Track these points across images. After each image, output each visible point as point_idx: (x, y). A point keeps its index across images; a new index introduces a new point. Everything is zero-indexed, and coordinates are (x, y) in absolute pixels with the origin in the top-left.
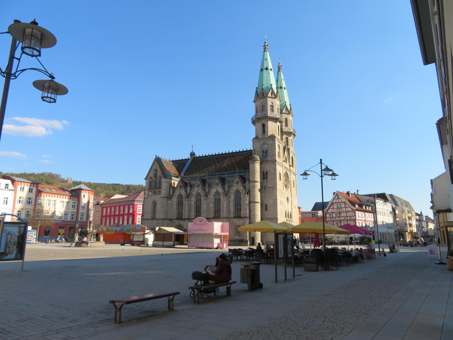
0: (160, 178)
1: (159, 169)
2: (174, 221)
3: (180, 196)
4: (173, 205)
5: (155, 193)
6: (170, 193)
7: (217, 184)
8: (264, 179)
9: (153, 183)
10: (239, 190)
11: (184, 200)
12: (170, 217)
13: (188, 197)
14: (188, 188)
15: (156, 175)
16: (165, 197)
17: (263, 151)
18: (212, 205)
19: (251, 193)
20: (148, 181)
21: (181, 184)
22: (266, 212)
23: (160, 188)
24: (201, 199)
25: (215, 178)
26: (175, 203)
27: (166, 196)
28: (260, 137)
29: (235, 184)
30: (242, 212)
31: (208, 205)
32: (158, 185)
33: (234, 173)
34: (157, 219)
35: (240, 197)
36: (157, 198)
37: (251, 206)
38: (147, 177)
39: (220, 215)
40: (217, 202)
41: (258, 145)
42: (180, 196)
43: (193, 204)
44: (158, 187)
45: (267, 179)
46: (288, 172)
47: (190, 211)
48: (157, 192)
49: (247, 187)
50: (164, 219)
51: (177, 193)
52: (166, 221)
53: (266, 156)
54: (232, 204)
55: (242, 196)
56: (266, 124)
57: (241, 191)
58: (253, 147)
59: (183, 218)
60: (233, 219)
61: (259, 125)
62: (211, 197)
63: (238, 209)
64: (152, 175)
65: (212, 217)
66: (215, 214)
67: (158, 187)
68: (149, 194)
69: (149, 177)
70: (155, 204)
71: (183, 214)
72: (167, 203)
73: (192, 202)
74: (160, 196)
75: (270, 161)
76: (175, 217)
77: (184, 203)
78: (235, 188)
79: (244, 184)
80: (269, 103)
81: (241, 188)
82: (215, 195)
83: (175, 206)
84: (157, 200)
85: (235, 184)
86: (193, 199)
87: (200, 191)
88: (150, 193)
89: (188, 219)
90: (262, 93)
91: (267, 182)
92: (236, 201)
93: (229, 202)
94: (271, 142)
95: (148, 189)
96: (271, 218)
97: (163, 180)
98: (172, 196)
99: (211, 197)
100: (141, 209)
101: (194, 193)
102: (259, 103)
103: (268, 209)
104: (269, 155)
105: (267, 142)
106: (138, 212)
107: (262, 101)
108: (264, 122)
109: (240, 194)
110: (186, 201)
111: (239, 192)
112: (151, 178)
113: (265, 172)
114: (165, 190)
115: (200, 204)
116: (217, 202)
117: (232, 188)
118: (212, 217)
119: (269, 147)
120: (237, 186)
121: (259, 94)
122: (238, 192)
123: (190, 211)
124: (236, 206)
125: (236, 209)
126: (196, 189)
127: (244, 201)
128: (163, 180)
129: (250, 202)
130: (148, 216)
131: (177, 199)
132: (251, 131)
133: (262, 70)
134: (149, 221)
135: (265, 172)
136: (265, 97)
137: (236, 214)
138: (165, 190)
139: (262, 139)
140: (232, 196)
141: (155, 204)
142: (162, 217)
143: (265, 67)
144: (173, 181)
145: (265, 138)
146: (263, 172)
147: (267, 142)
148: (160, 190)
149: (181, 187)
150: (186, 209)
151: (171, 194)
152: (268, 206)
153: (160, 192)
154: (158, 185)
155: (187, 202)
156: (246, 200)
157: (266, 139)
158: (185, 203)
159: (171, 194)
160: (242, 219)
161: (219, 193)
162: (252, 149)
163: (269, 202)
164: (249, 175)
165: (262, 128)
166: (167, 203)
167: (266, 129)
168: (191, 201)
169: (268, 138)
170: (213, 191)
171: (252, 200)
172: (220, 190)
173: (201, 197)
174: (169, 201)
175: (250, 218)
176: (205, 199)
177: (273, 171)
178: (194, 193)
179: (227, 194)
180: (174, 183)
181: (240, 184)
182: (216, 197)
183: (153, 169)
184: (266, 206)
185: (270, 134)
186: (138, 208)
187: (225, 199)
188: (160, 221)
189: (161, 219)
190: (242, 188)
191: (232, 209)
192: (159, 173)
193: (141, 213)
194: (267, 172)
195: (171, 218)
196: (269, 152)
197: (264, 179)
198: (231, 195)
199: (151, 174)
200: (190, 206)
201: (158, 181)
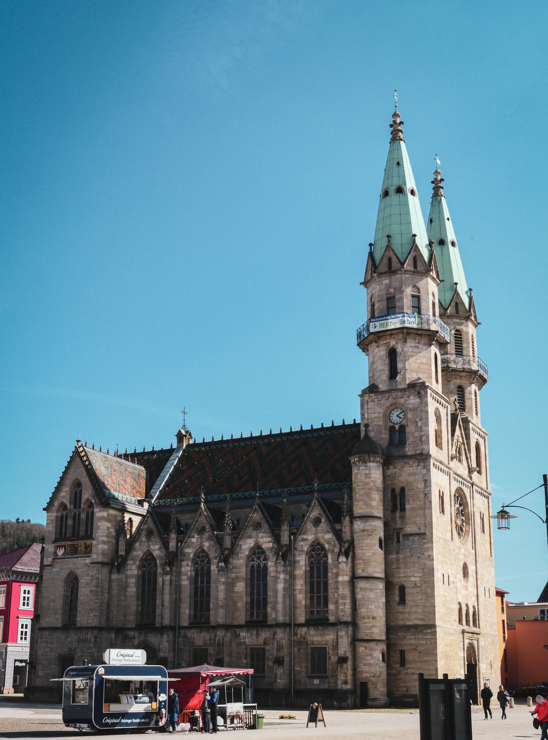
0: (91, 506)
1: (85, 481)
2: (131, 633)
3: (149, 558)
4: (127, 586)
5: (74, 552)
6: (117, 551)
7: (257, 526)
8: (394, 510)
9: (70, 522)
10: (322, 541)
11: (159, 570)
12: (117, 622)
13: (170, 564)
14: (173, 536)
15: (76, 497)
16: (103, 564)
17: (392, 429)
18: (240, 587)
19: (358, 552)
21: (150, 524)
22: (401, 608)
23: (89, 535)
24: (209, 569)
25: (251, 507)
26: (133, 581)
27: (105, 560)
28: (382, 387)
29: (309, 525)
30: (331, 607)
31: (230, 586)
32: (82, 528)
33: (306, 493)
34: (80, 629)
35: (326, 562)
36: (80, 565)
37: (358, 590)
38: (50, 504)
39: (265, 615)
40: (258, 578)
41: (376, 411)
42: (149, 558)
43: (185, 583)
44: (82, 533)
45: (403, 509)
46: (464, 488)
47: (176, 603)
48: (82, 548)
49: (347, 536)
50: (100, 629)
51: (139, 552)
52: (105, 634)
53: (402, 442)
54: (300, 584)
55: (330, 561)
56: (399, 350)
57: (326, 546)
58: (363, 415)
59: (158, 625)
60: (304, 629)
61: (380, 352)
62: (240, 562)
63: (319, 597)
64: (65, 496)
65: (243, 622)
66: (252, 614)
67: (82, 533)
68: (55, 554)
69: (56, 504)
70: (73, 581)
71: (158, 612)
72: (110, 581)
73: (184, 577)
74: (88, 561)
75: (411, 457)
76: (132, 620)
77: (160, 580)
78: (310, 537)
79: (338, 527)
80: (409, 291)
81: (327, 537)
82: (250, 558)
83: (132, 590)
84: (79, 572)
85: (309, 525)
86: (187, 569)
87: (206, 544)
88: (60, 552)
89: (171, 628)
90: (385, 261)
91: (403, 518)
92: (312, 576)
93: (292, 577)
94: (413, 401)
95: (53, 537)
96: (416, 627)
97: (100, 513)
98: (125, 559)
99: (240, 562)
100: (32, 596)
101: (190, 551)
102: (379, 287)
103: (408, 598)
104: (410, 440)
105: (402, 401)
106: (21, 607)
107: (386, 281)
108: (393, 343)
109: (326, 556)
110: (166, 573)
111: (323, 548)
112: (63, 506)
113: (398, 491)
114: (104, 542)
115: (209, 582)
116: (258, 578)
117: (300, 537)
118: (243, 622)
119: (410, 415)
120: (316, 533)
121: (377, 261)
122: (317, 549)
123: (176, 603)
124: (312, 591)
125: (312, 598)
126: (194, 540)
127: (337, 575)
128: (100, 513)
129: (354, 578)
130: (54, 619)
131: (139, 568)
132: (359, 369)
133: (386, 194)
134: (58, 634)
135: (398, 491)
136: (395, 272)
137: (312, 612)
138: (104, 542)
139: (389, 391)
140: (302, 560)
141: (73, 581)
142: (95, 623)
143: (396, 183)
144: (127, 516)
145: (397, 390)
146: (393, 490)
147: (402, 401)
148: (88, 542)
149: (150, 534)
150: (167, 597)
151: (122, 553)
152: (407, 591)
153: (88, 550)
154: (82, 528)
155: (168, 578)
156: (340, 572)
157: (399, 394)
158: (164, 580)
159: (122, 553)
160: (330, 628)
161: (263, 552)
162: (358, 421)
163: (410, 576)
164: (351, 498)
165: (387, 361)
166: (110, 581)
167: (400, 365)
168: (179, 573)
169: (404, 390)
170: (247, 545)
171: (359, 572)
172: (266, 542)
173: (209, 562)
174: (114, 576)
175: (354, 624)
176: (221, 570)
177: (421, 486)
178: (190, 551)
179: (285, 554)
180: (130, 520)
181: (324, 525)
182: (255, 564)
183: (69, 482)
184: (402, 589)
185: (411, 377)
186: (22, 595)
187: (281, 569)
188: (89, 635)
189: (93, 628)
190: (329, 536)
191: (301, 598)
192: (87, 494)
193: (31, 608)
194: (403, 490)
195: (120, 625)
196: (408, 429)
197: (394, 510)
198: (298, 558)
199: (62, 494)
200: (177, 589)
201: (83, 516)
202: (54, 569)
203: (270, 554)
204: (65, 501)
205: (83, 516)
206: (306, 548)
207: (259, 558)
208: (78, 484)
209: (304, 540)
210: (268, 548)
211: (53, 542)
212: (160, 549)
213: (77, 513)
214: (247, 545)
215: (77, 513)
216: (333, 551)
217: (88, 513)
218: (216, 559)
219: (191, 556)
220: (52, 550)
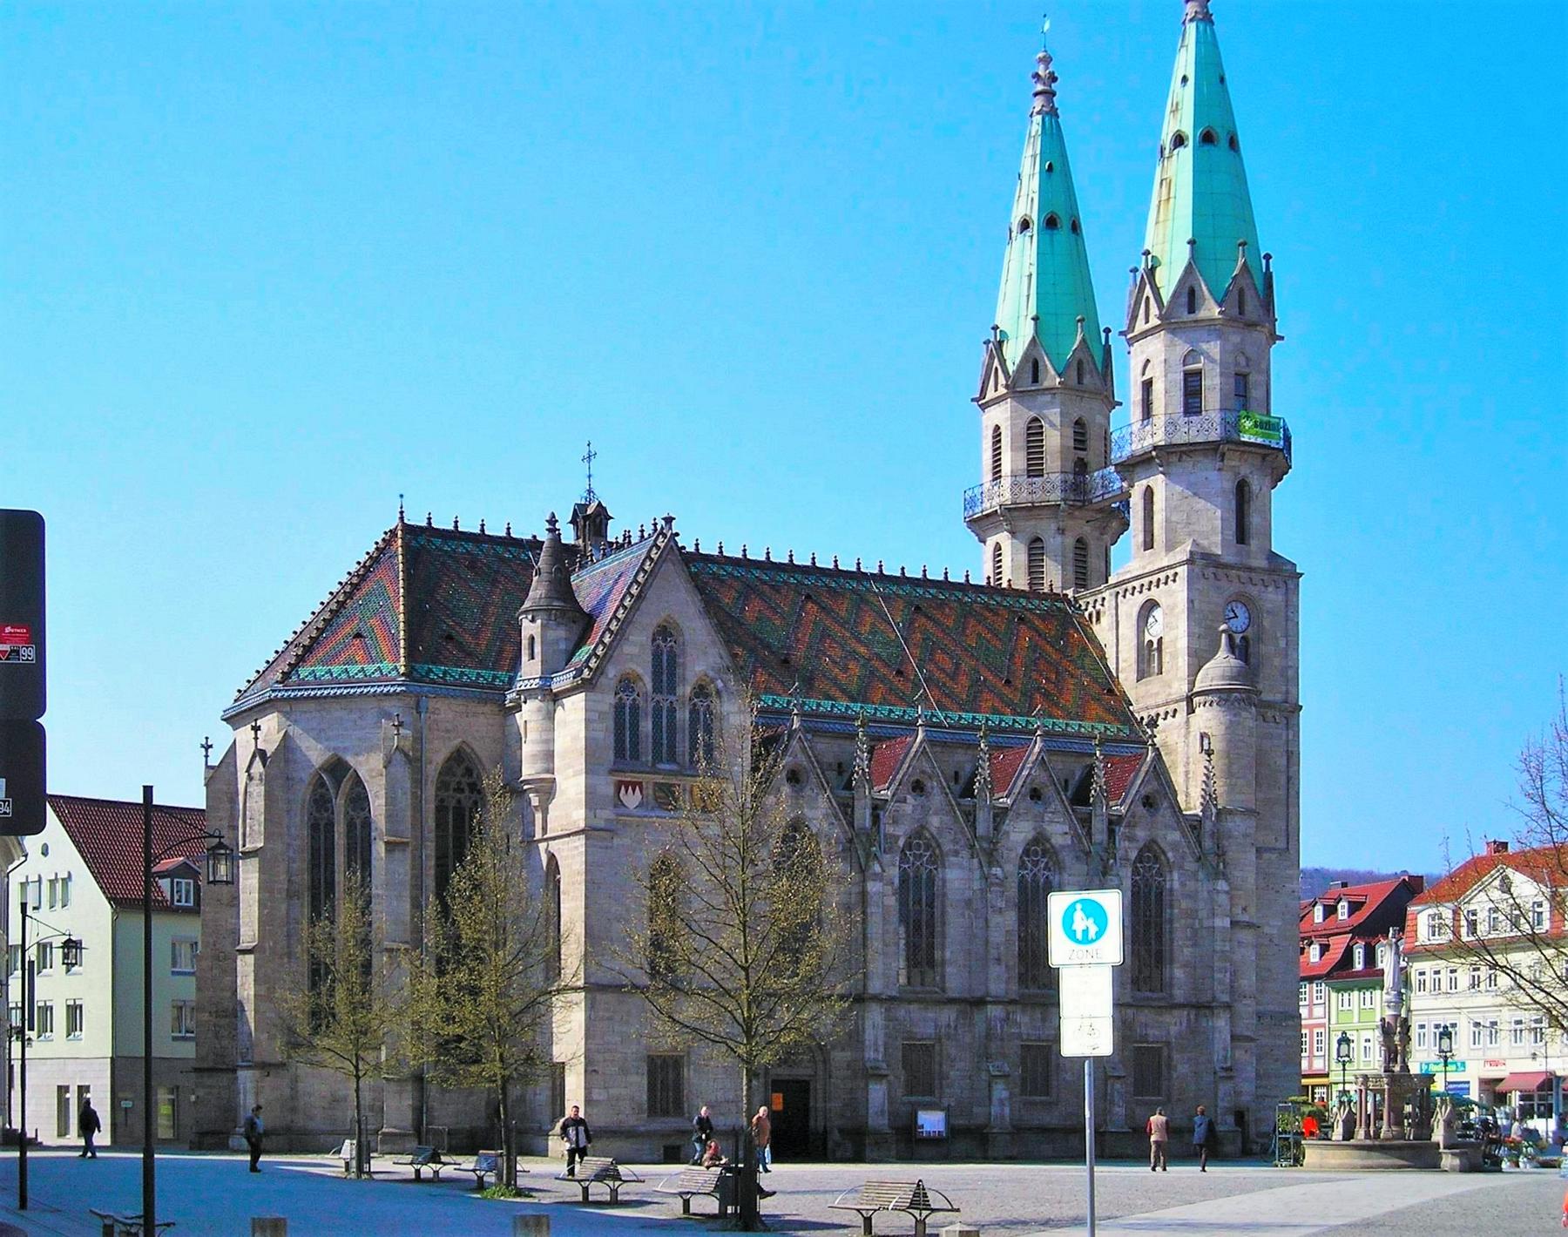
5: (665, 798)
9: (647, 726)
15: (666, 667)
20: (608, 701)
57: (1170, 855)
69: (612, 672)
78: (1141, 834)
87: (935, 822)
88: (632, 799)
94: (1272, 597)
105: (1254, 591)
108: (1244, 470)
112: (627, 683)
130: (630, 964)
199: (628, 649)
201: (683, 715)
202: (616, 841)
203: (1067, 858)
204: (640, 671)
205: (683, 715)
206: (1133, 855)
207: (1036, 864)
208: (664, 632)
209: (1131, 839)
210: (1063, 847)
211: (612, 772)
212: (826, 816)
213: (665, 705)
214: (1019, 833)
215: (665, 705)
216: (1181, 867)
217: (694, 711)
218: (956, 853)
219: (901, 843)
220: (611, 790)
